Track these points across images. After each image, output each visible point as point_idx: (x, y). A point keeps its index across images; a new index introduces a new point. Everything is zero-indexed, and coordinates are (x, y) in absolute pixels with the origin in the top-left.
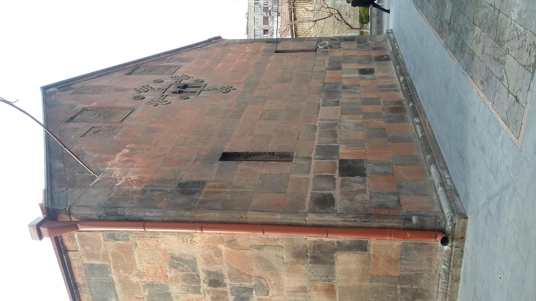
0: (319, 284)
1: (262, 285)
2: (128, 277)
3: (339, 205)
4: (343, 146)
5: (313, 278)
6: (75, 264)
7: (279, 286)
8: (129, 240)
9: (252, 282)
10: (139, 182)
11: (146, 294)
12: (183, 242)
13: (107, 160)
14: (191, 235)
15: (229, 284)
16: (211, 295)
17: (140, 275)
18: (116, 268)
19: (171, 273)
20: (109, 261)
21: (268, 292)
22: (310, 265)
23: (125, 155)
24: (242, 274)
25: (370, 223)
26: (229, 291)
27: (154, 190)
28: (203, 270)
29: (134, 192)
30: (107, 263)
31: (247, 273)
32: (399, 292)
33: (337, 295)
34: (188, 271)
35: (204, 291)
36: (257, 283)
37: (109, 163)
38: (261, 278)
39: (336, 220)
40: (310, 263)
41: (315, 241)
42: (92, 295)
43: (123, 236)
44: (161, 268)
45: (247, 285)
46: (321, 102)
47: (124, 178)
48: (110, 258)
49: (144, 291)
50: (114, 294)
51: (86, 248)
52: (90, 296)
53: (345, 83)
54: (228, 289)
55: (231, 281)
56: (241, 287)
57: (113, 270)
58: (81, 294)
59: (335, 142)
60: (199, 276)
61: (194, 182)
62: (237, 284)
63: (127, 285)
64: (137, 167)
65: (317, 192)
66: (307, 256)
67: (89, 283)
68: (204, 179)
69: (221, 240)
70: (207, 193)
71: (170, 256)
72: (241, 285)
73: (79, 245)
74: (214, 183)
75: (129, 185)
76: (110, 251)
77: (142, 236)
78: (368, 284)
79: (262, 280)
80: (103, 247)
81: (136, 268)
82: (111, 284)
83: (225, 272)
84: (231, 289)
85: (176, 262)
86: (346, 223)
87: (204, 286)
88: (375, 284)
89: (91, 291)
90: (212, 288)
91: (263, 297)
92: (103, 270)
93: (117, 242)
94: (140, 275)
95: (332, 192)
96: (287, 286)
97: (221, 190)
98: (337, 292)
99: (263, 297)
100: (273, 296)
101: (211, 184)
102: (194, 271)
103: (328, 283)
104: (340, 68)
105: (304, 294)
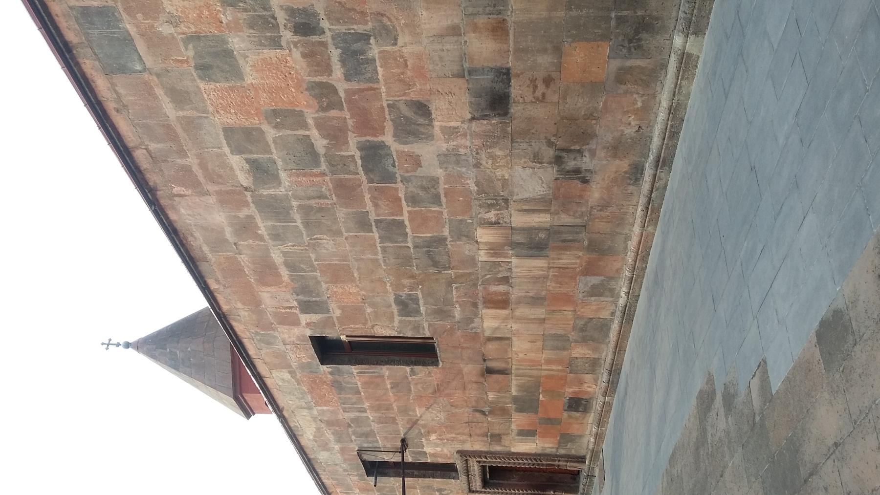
0: (481, 20)
1: (385, 27)
2: (153, 26)
5: (470, 10)
7: (413, 27)
9: (366, 24)
11: (191, 53)
15: (329, 29)
16: (301, 49)
17: (174, 21)
18: (129, 10)
19: (227, 16)
21: (396, 39)
24: (350, 10)
26: (330, 41)
28: (281, 7)
31: (358, 9)
32: (613, 23)
33: (511, 37)
34: (255, 11)
35: (288, 43)
36: (376, 25)
38: (383, 15)
42: (99, 60)
44: (208, 6)
45: (360, 28)
50: (136, 58)
52: (97, 63)
54: (328, 37)
55: (332, 24)
56: (350, 33)
57: (125, 16)
58: (80, 60)
60: (275, 19)
62: (343, 29)
63: (155, 41)
67: (88, 41)
78: (563, 14)
79: (385, 20)
82: (127, 41)
83: (320, 8)
84: (333, 38)
87: (287, 35)
88: (574, 13)
89: (95, 54)
90: (300, 38)
91: (388, 48)
94: (174, 21)
96: (428, 26)
98: (511, 32)
99: (388, 48)
100: (405, 45)
102: (265, 9)
103: (495, 16)
105: (455, 38)
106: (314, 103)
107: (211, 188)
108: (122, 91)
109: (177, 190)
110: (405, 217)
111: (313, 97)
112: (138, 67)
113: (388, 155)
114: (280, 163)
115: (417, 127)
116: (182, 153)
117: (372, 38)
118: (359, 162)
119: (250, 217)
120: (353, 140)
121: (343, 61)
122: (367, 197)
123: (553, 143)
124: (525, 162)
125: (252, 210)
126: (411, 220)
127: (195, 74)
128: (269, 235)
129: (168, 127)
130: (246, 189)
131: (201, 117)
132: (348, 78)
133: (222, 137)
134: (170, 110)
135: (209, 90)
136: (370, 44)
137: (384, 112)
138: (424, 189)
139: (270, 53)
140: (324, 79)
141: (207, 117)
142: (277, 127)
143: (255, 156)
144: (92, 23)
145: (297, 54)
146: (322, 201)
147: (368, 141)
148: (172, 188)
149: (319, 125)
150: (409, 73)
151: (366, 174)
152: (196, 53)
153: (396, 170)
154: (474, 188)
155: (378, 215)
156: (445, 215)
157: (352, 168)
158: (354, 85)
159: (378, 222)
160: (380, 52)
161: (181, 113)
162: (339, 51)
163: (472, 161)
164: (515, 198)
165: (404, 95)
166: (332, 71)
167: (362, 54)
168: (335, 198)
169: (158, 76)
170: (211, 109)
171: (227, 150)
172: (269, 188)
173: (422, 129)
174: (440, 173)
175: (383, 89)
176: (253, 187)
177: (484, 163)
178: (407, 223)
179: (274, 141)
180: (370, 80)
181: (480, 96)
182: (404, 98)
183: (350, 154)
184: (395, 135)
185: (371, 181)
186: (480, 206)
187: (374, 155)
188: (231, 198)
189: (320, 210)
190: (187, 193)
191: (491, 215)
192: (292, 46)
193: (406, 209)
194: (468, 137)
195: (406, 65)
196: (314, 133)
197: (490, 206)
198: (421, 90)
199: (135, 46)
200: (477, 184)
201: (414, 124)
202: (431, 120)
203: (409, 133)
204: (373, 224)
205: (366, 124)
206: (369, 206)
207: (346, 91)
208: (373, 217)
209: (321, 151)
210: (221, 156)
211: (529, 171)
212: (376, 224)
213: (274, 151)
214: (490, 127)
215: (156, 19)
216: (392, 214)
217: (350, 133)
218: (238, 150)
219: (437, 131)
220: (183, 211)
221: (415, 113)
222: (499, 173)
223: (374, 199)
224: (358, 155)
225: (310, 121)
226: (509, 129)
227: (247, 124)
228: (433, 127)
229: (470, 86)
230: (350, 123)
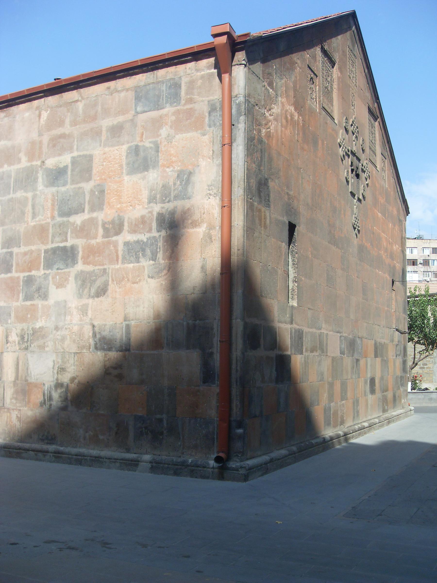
2: (167, 124)
3: (251, 353)
4: (303, 359)
6: (181, 68)
8: (210, 126)
10: (268, 135)
11: (147, 144)
12: (208, 186)
13: (287, 97)
14: (215, 195)
16: (147, 215)
17: (169, 139)
18: (178, 112)
19: (171, 173)
20: (185, 104)
21: (152, 277)
22: (185, 323)
23: (292, 115)
25: (235, 387)
27: (262, 153)
29: (260, 131)
30: (183, 102)
32: (158, 416)
33: (152, 352)
34: (174, 190)
37: (284, 100)
39: (238, 351)
40: (188, 324)
41: (212, 329)
42: (145, 86)
43: (214, 121)
46: (344, 335)
47: (271, 118)
48: (188, 106)
49: (150, 142)
50: (146, 109)
51: (200, 81)
53: (362, 362)
56: (157, 248)
59: (306, 351)
60: (169, 202)
61: (269, 195)
63: (157, 124)
64: (282, 131)
65: (262, 331)
66: (196, 320)
68: (272, 206)
69: (211, 227)
70: (260, 211)
71: (192, 171)
72: (160, 248)
73: (203, 73)
74: (268, 218)
75: (266, 125)
76: (196, 106)
77: (215, 141)
80: (201, 99)
81: (178, 134)
82: (158, 107)
85: (186, 178)
86: (234, 362)
92: (175, 97)
93: (207, 114)
94: (169, 139)
95: (262, 346)
97: (263, 225)
98: (155, 352)
101: (268, 214)
104: (376, 356)
106: (110, 218)
107: (46, 139)
108: (123, 94)
109: (45, 115)
110: (14, 274)
111: (113, 219)
112: (139, 109)
113: (67, 265)
114: (63, 189)
115: (88, 287)
116: (74, 123)
117: (154, 262)
118: (62, 245)
119: (19, 161)
120: (80, 243)
121: (138, 242)
122: (33, 248)
123: (73, 381)
124: (58, 362)
125: (24, 163)
126: (11, 278)
127: (132, 144)
128: (3, 172)
129: (94, 118)
130: (43, 162)
131: (101, 141)
132: (127, 244)
133: (85, 153)
134: (106, 123)
135: (120, 152)
136: (149, 261)
137: (100, 265)
138: (39, 289)
139: (145, 195)
140: (126, 227)
141: (100, 146)
142: (92, 192)
143: (69, 173)
144: (170, 87)
145: (144, 212)
146: (30, 215)
147: (78, 253)
148: (46, 111)
149: (92, 221)
150: (128, 285)
151: (52, 249)
152: (147, 147)
153: (55, 271)
154: (38, 325)
155: (17, 254)
156: (15, 304)
157: (57, 239)
158: (121, 247)
159: (11, 254)
160: (144, 267)
161: (104, 129)
162: (145, 240)
163: (61, 324)
164: (29, 355)
165: (113, 280)
166: (131, 233)
167: (143, 255)
168: (32, 224)
169: (132, 120)
170: (107, 149)
171: (75, 154)
172: (43, 179)
173: (86, 290)
174: (51, 301)
175: (117, 267)
176: (44, 167)
177: (59, 333)
178: (9, 275)
179: (80, 188)
180: (124, 258)
181: (110, 332)
182: (110, 280)
183: (69, 239)
184: (82, 272)
185: (46, 251)
186: (23, 329)
187: (68, 255)
188: (34, 150)
189: (23, 213)
190: (42, 120)
191: (14, 337)
192: (150, 210)
193: (22, 275)
194: (79, 323)
195: (134, 283)
196: (85, 216)
197: (22, 337)
198: (116, 292)
199: (154, 110)
200: (41, 328)
201: (91, 286)
202: (93, 297)
203: (84, 281)
204: (9, 250)
205: (92, 252)
206: (23, 249)
207: (117, 242)
208: (15, 250)
209: (72, 219)
210: (71, 149)
211: (51, 364)
212: (9, 252)
213: (73, 186)
214: (87, 337)
215: (171, 127)
216: (17, 264)
217: (85, 240)
218: (74, 161)
219: (85, 301)
220: (27, 114)
221: (99, 287)
222: (50, 344)
223: (31, 252)
224: (68, 244)
225: (95, 215)
226: (85, 351)
227: (94, 171)
228: (88, 298)
229: (118, 325)
230: (93, 242)
